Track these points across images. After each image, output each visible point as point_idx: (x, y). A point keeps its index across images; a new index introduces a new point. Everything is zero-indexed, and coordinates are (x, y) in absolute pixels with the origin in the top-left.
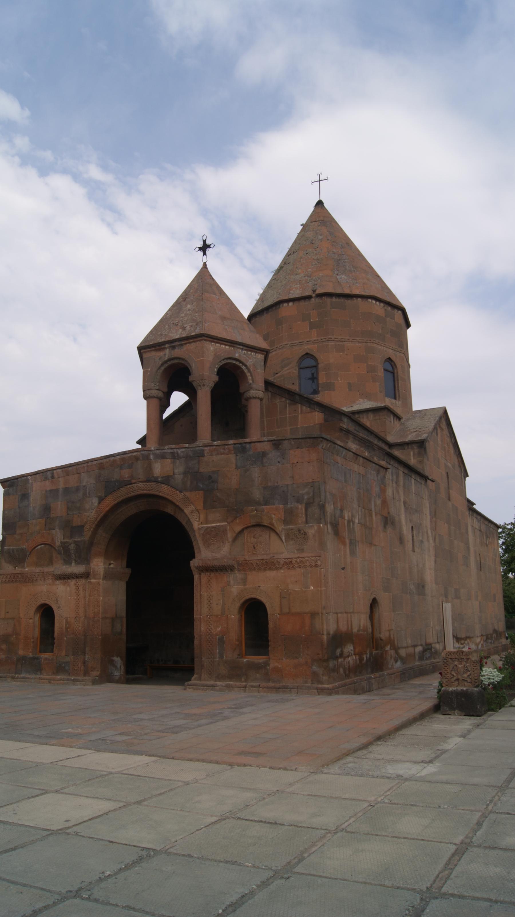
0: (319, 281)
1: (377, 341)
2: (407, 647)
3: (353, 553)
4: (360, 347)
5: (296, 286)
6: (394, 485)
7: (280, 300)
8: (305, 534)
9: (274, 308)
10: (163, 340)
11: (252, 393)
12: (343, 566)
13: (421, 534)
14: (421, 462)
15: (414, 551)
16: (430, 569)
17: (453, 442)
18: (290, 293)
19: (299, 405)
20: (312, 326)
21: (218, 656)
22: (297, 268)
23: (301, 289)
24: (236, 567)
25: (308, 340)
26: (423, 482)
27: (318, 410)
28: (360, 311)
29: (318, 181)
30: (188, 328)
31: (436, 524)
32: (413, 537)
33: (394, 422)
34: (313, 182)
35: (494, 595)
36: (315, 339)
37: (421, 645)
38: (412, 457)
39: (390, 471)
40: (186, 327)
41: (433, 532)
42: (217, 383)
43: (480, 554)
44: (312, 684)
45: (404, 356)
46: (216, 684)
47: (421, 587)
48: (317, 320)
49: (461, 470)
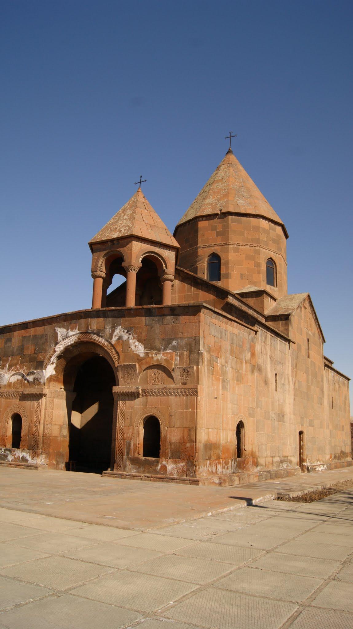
0: (224, 204)
1: (262, 246)
2: (267, 457)
3: (224, 388)
4: (250, 250)
5: (209, 207)
6: (263, 344)
7: (197, 216)
8: (188, 372)
9: (193, 221)
10: (106, 239)
11: (166, 276)
12: (216, 396)
13: (283, 379)
14: (287, 330)
15: (276, 390)
16: (289, 404)
17: (314, 318)
18: (204, 211)
19: (200, 286)
20: (218, 234)
21: (126, 454)
22: (210, 195)
23: (212, 209)
24: (141, 393)
25: (215, 244)
26: (287, 343)
27: (212, 290)
28: (252, 225)
29: (229, 137)
30: (123, 231)
31: (296, 373)
32: (276, 381)
33: (271, 301)
34: (226, 138)
35: (343, 427)
36: (219, 243)
37: (279, 457)
38: (281, 326)
39: (259, 333)
40: (122, 231)
41: (294, 379)
42: (141, 268)
43: (332, 397)
44: (186, 477)
45: (282, 257)
46: (123, 474)
47: (281, 416)
48: (222, 230)
49: (320, 338)
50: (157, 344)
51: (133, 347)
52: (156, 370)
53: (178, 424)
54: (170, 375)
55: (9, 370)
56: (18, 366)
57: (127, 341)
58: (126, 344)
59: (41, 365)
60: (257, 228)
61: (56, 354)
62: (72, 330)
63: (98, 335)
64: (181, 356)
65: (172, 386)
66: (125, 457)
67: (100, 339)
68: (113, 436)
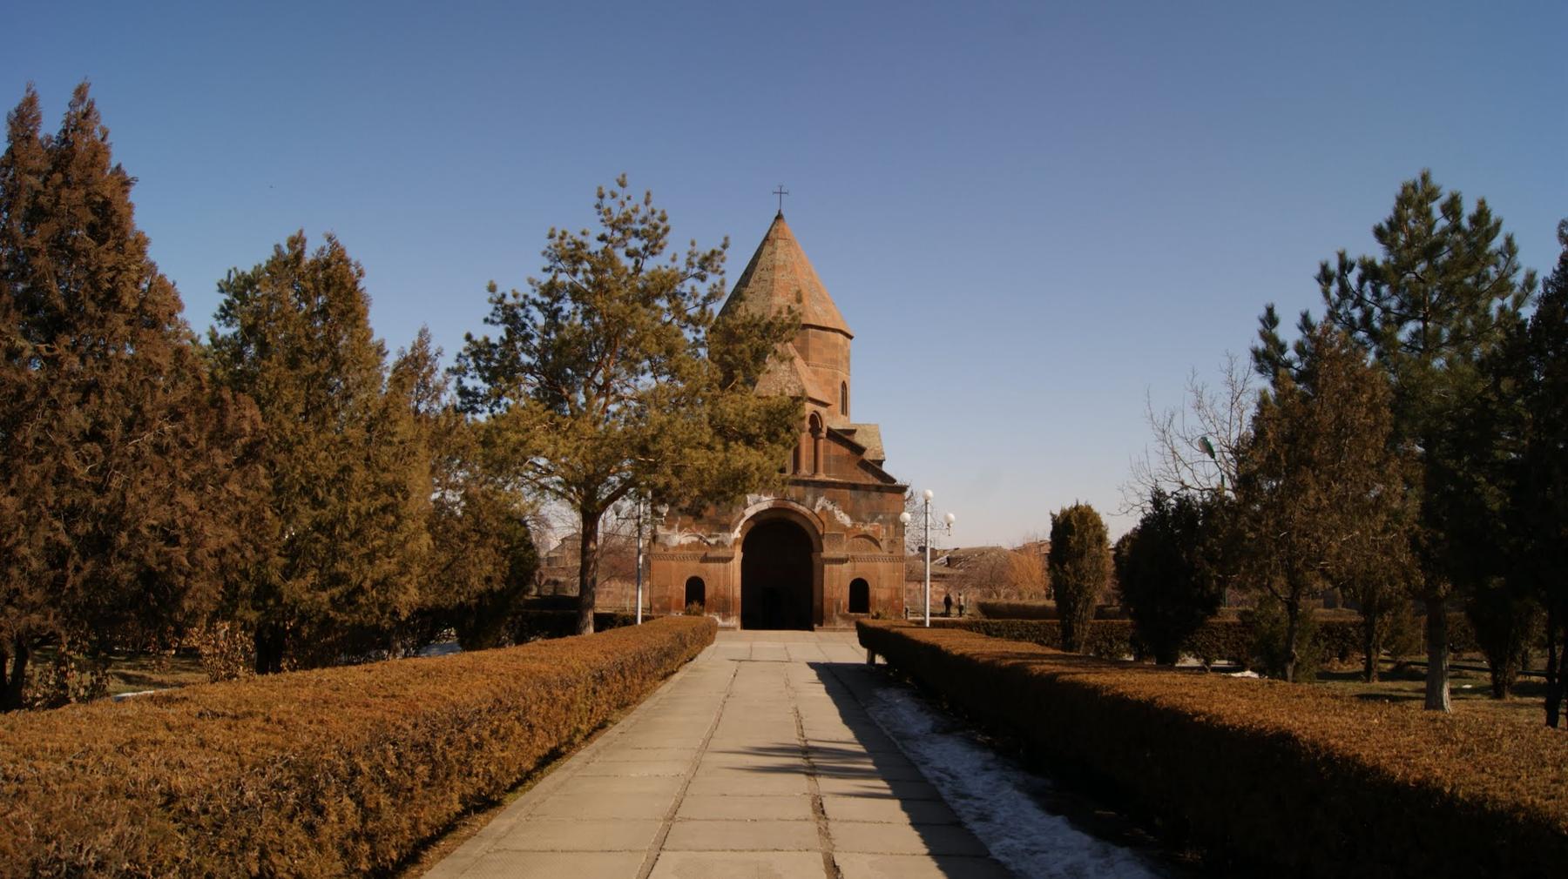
50: (864, 516)
51: (838, 518)
52: (862, 539)
53: (886, 585)
54: (877, 544)
55: (680, 529)
56: (694, 528)
57: (833, 511)
58: (831, 515)
59: (727, 528)
60: (835, 346)
61: (745, 519)
62: (765, 496)
63: (798, 503)
64: (887, 529)
65: (880, 553)
66: (834, 614)
67: (801, 507)
68: (817, 595)
